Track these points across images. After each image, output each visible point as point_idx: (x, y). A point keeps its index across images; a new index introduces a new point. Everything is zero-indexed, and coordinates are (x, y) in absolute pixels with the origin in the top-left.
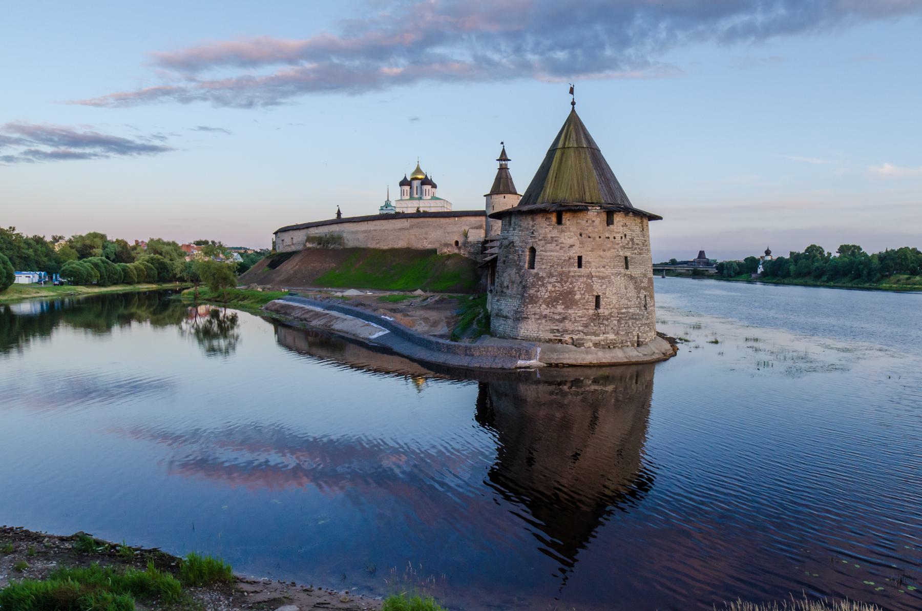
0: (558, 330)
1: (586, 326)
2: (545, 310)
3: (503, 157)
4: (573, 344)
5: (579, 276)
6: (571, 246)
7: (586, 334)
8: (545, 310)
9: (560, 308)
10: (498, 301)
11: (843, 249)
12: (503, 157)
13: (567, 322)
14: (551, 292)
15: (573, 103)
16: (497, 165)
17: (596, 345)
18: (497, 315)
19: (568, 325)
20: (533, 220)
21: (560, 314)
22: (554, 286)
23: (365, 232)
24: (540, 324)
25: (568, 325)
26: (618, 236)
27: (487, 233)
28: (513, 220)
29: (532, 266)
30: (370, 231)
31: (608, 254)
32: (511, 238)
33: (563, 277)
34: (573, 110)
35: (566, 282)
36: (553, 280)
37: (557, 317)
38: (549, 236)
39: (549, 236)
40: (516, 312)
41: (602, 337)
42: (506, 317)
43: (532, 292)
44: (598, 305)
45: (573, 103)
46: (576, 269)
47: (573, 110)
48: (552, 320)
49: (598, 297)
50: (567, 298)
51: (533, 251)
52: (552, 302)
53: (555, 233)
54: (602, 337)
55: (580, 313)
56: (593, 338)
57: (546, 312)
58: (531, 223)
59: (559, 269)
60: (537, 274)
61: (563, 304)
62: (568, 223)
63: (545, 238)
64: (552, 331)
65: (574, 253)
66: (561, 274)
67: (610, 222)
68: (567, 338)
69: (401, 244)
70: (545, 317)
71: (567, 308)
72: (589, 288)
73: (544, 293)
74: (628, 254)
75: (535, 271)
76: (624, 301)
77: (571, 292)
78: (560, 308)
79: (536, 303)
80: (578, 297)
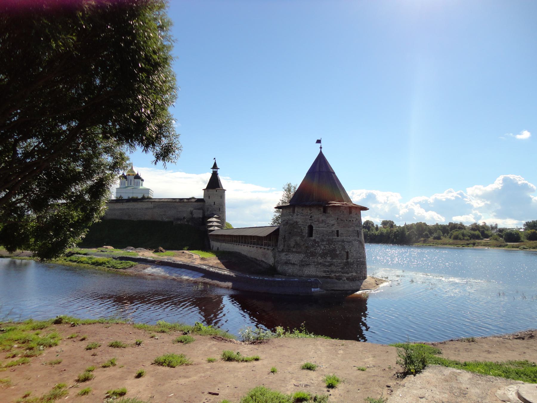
0: (328, 271)
1: (342, 268)
2: (321, 260)
3: (215, 167)
4: (336, 279)
5: (339, 241)
6: (333, 225)
7: (343, 273)
8: (321, 260)
9: (329, 259)
10: (286, 255)
11: (385, 223)
12: (215, 167)
13: (333, 266)
14: (323, 250)
15: (321, 148)
16: (211, 171)
17: (348, 279)
18: (286, 263)
19: (334, 268)
20: (311, 210)
21: (329, 262)
22: (325, 247)
23: (121, 209)
24: (317, 268)
25: (334, 268)
26: (354, 219)
27: (204, 213)
28: (296, 209)
29: (310, 234)
30: (124, 209)
31: (350, 229)
32: (295, 220)
33: (330, 242)
34: (321, 152)
35: (331, 244)
36: (325, 243)
37: (327, 264)
38: (321, 219)
39: (321, 219)
40: (302, 261)
41: (350, 275)
42: (294, 264)
43: (311, 250)
44: (347, 258)
45: (321, 148)
46: (336, 237)
47: (321, 152)
48: (324, 265)
49: (347, 252)
50: (333, 253)
51: (311, 228)
52: (324, 255)
53: (324, 218)
54: (350, 275)
55: (339, 261)
56: (346, 275)
57: (321, 261)
58: (309, 212)
59: (327, 237)
60: (315, 240)
61: (330, 256)
62: (331, 213)
63: (318, 221)
64: (325, 272)
65: (334, 229)
66: (328, 240)
67: (350, 212)
68: (333, 275)
69: (148, 217)
70: (320, 263)
71: (332, 258)
72: (344, 248)
73: (319, 251)
74: (358, 229)
75: (313, 238)
76: (359, 255)
77: (335, 250)
78: (329, 259)
79: (315, 256)
80: (338, 252)
